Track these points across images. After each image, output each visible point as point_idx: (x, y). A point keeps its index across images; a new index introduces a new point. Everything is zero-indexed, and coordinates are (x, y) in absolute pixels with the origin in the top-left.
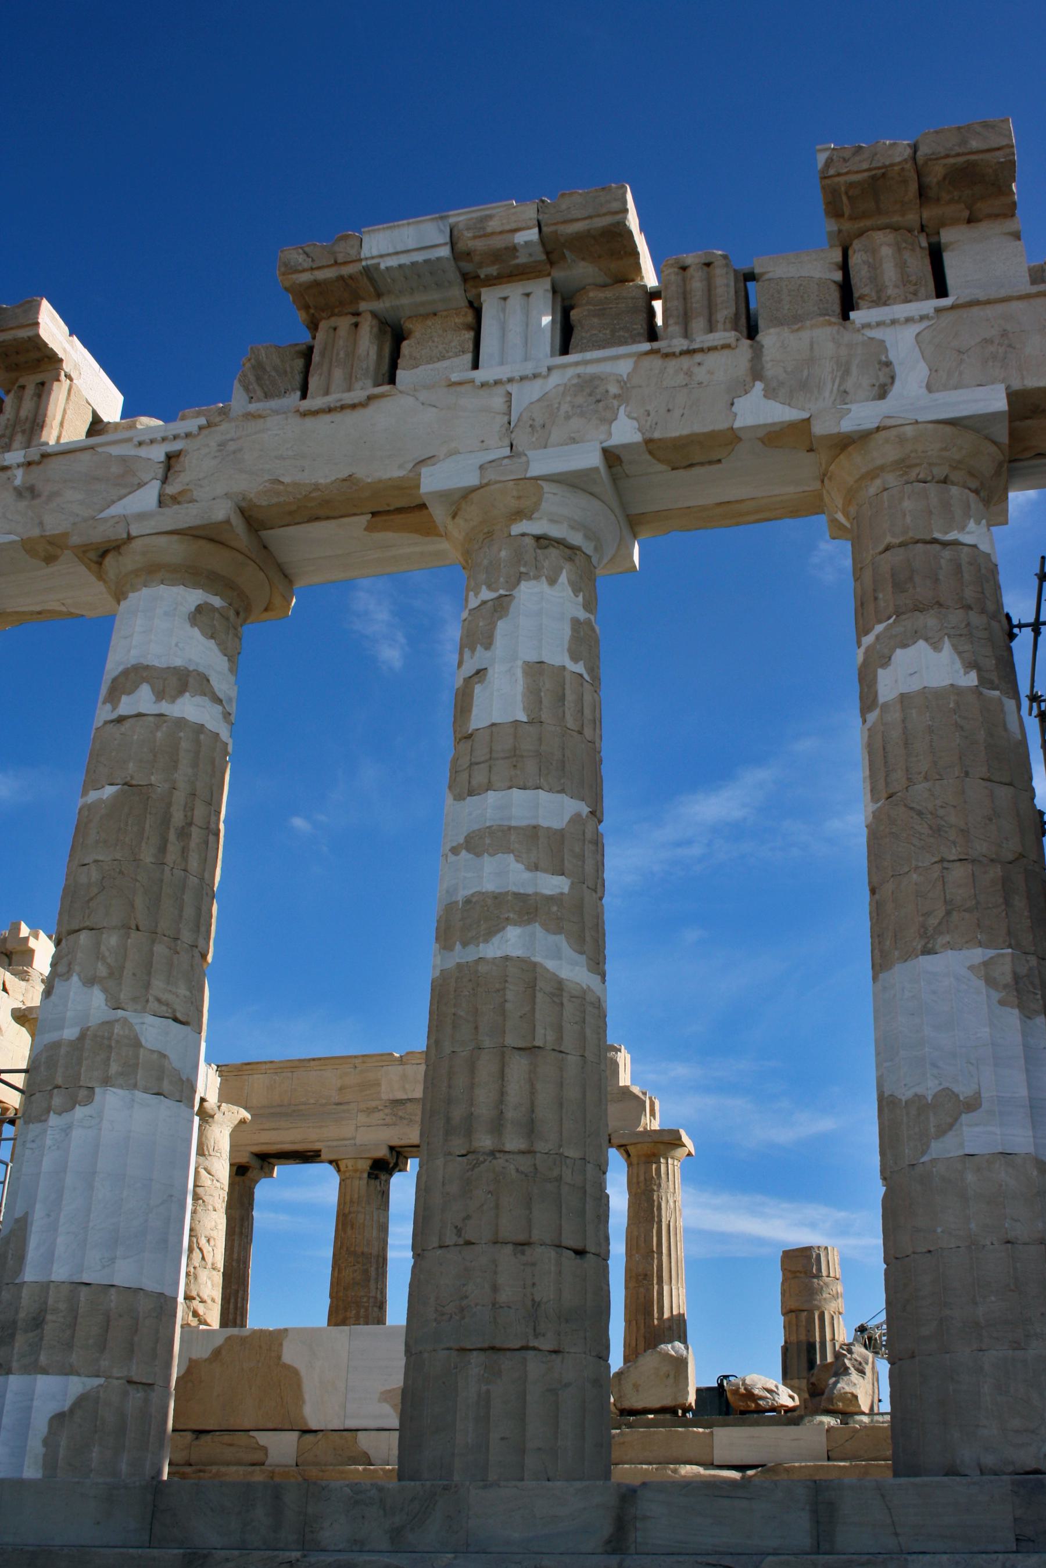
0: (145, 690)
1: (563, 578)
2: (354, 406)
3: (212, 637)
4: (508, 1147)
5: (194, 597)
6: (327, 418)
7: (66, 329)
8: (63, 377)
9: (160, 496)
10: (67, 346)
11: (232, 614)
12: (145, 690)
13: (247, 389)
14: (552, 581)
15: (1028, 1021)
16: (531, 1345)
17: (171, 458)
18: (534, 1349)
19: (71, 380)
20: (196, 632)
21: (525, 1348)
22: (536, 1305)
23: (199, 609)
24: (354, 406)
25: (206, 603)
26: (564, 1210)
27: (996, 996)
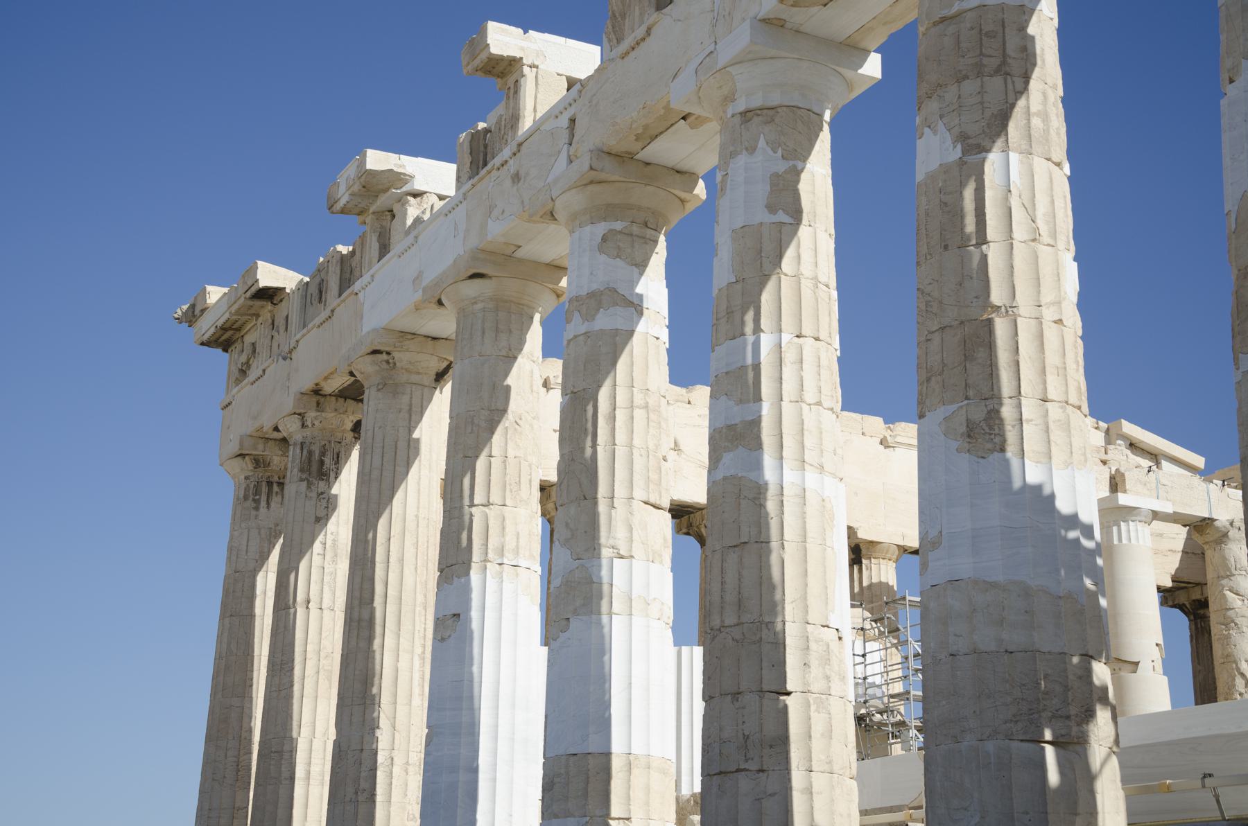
0: (577, 318)
1: (762, 143)
2: (643, 39)
3: (618, 256)
4: (727, 623)
5: (601, 228)
6: (633, 54)
7: (520, 31)
8: (526, 70)
9: (569, 156)
10: (525, 44)
11: (635, 229)
12: (577, 318)
13: (610, 40)
14: (752, 150)
15: (981, 460)
16: (742, 767)
17: (573, 121)
18: (745, 770)
19: (537, 67)
20: (603, 258)
21: (738, 770)
22: (746, 738)
23: (604, 239)
24: (643, 39)
25: (611, 230)
26: (765, 664)
27: (954, 445)
